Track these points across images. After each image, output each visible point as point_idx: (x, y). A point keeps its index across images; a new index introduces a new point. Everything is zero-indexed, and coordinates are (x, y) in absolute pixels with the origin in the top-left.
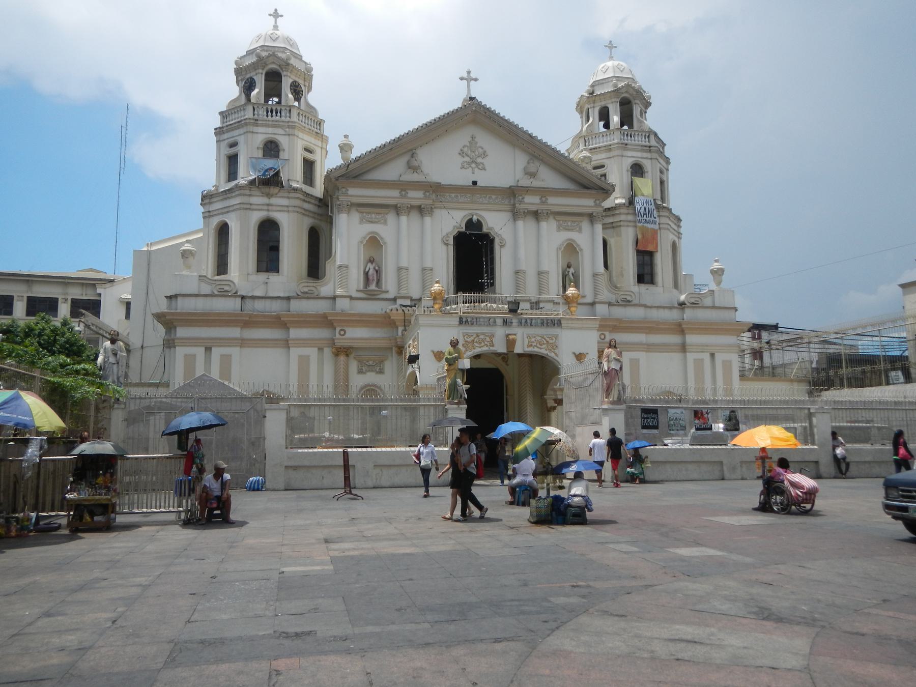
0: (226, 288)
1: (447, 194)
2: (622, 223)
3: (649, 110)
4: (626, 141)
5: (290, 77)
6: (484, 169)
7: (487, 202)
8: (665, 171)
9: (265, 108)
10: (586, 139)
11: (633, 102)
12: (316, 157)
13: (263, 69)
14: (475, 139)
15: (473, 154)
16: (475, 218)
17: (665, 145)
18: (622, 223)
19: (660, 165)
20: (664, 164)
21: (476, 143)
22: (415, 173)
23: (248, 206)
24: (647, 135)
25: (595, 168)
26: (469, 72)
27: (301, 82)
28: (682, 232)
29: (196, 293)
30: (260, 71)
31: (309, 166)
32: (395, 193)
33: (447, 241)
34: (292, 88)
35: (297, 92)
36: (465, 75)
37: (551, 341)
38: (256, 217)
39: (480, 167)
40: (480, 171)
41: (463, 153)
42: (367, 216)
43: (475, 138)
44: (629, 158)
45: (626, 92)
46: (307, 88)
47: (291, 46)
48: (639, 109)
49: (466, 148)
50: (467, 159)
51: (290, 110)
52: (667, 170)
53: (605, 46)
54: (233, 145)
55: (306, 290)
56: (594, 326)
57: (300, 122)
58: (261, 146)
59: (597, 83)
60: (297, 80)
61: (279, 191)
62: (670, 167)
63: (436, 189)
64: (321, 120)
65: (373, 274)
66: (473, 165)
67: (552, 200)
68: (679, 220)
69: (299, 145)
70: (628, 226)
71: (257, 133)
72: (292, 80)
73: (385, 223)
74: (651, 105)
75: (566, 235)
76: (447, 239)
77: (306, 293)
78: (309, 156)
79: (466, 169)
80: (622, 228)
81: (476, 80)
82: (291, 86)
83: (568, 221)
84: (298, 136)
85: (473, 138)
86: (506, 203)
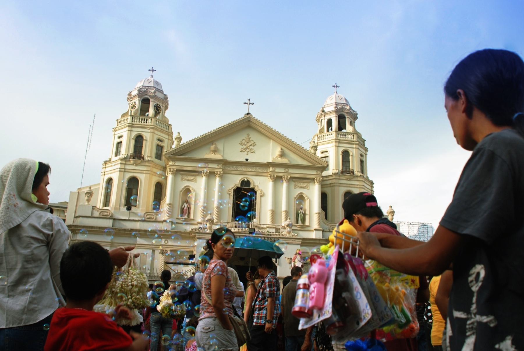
0: (106, 214)
1: (231, 166)
2: (335, 184)
3: (356, 121)
4: (340, 138)
5: (154, 102)
7: (254, 171)
8: (364, 155)
9: (138, 118)
10: (319, 136)
11: (346, 116)
12: (165, 144)
13: (141, 98)
14: (249, 136)
15: (248, 144)
16: (246, 180)
17: (365, 140)
18: (335, 184)
19: (361, 152)
20: (364, 152)
21: (250, 138)
22: (214, 154)
23: (123, 170)
24: (353, 135)
25: (322, 153)
27: (161, 104)
28: (374, 190)
29: (90, 215)
30: (140, 99)
31: (160, 148)
33: (230, 192)
34: (155, 107)
35: (157, 109)
36: (247, 101)
38: (128, 175)
39: (252, 151)
40: (251, 153)
41: (242, 143)
42: (185, 177)
43: (249, 135)
44: (342, 148)
45: (342, 111)
46: (164, 107)
47: (158, 85)
49: (244, 141)
50: (245, 147)
51: (152, 119)
52: (366, 154)
53: (333, 86)
54: (120, 137)
55: (148, 216)
56: (299, 242)
57: (157, 126)
58: (134, 138)
59: (326, 106)
60: (159, 103)
61: (141, 162)
62: (368, 153)
63: (225, 163)
64: (169, 124)
65: (186, 209)
66: (248, 150)
67: (291, 171)
68: (372, 183)
69: (156, 137)
70: (339, 186)
71: (133, 131)
72: (156, 104)
73: (196, 181)
74: (357, 119)
75: (298, 191)
76: (229, 191)
77: (148, 218)
78: (160, 143)
79: (243, 152)
80: (336, 187)
81: (253, 104)
82: (155, 106)
83: (302, 182)
84: (154, 133)
86: (265, 171)
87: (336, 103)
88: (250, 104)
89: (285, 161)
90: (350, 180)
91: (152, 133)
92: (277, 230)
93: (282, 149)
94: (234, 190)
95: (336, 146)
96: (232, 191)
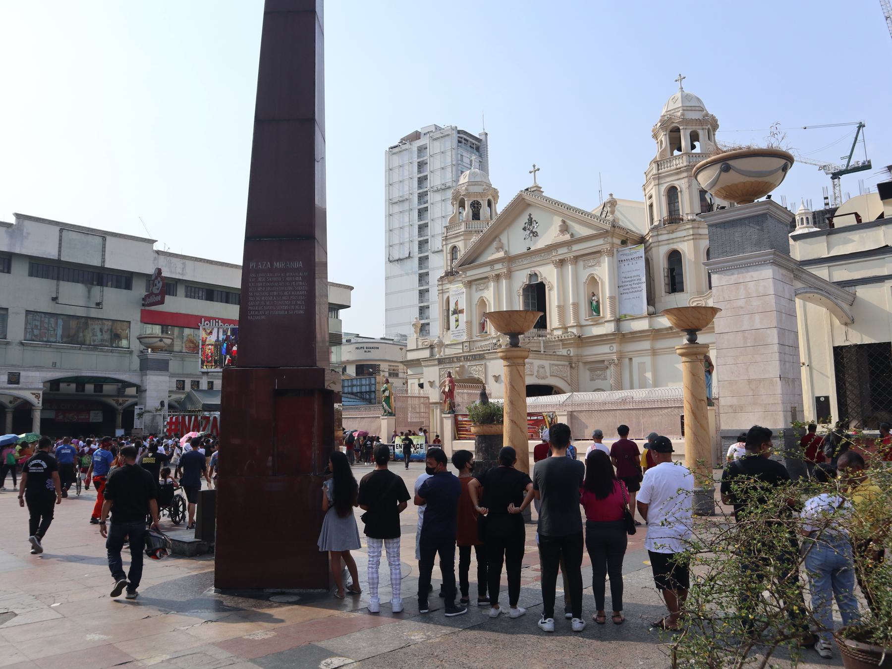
0: (426, 343)
6: (537, 235)
23: (441, 291)
26: (534, 166)
32: (488, 269)
35: (476, 206)
36: (532, 169)
37: (481, 369)
45: (673, 122)
48: (688, 132)
60: (475, 199)
63: (510, 260)
67: (575, 247)
70: (659, 246)
82: (471, 205)
85: (530, 215)
87: (666, 112)
88: (535, 171)
89: (567, 237)
90: (673, 232)
91: (463, 241)
92: (565, 328)
93: (564, 222)
94: (524, 290)
95: (655, 185)
96: (521, 291)
